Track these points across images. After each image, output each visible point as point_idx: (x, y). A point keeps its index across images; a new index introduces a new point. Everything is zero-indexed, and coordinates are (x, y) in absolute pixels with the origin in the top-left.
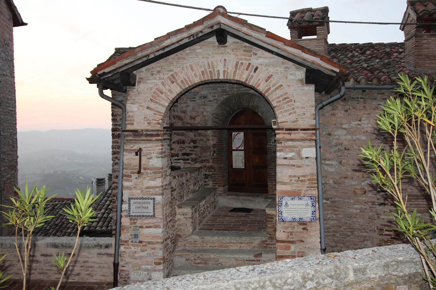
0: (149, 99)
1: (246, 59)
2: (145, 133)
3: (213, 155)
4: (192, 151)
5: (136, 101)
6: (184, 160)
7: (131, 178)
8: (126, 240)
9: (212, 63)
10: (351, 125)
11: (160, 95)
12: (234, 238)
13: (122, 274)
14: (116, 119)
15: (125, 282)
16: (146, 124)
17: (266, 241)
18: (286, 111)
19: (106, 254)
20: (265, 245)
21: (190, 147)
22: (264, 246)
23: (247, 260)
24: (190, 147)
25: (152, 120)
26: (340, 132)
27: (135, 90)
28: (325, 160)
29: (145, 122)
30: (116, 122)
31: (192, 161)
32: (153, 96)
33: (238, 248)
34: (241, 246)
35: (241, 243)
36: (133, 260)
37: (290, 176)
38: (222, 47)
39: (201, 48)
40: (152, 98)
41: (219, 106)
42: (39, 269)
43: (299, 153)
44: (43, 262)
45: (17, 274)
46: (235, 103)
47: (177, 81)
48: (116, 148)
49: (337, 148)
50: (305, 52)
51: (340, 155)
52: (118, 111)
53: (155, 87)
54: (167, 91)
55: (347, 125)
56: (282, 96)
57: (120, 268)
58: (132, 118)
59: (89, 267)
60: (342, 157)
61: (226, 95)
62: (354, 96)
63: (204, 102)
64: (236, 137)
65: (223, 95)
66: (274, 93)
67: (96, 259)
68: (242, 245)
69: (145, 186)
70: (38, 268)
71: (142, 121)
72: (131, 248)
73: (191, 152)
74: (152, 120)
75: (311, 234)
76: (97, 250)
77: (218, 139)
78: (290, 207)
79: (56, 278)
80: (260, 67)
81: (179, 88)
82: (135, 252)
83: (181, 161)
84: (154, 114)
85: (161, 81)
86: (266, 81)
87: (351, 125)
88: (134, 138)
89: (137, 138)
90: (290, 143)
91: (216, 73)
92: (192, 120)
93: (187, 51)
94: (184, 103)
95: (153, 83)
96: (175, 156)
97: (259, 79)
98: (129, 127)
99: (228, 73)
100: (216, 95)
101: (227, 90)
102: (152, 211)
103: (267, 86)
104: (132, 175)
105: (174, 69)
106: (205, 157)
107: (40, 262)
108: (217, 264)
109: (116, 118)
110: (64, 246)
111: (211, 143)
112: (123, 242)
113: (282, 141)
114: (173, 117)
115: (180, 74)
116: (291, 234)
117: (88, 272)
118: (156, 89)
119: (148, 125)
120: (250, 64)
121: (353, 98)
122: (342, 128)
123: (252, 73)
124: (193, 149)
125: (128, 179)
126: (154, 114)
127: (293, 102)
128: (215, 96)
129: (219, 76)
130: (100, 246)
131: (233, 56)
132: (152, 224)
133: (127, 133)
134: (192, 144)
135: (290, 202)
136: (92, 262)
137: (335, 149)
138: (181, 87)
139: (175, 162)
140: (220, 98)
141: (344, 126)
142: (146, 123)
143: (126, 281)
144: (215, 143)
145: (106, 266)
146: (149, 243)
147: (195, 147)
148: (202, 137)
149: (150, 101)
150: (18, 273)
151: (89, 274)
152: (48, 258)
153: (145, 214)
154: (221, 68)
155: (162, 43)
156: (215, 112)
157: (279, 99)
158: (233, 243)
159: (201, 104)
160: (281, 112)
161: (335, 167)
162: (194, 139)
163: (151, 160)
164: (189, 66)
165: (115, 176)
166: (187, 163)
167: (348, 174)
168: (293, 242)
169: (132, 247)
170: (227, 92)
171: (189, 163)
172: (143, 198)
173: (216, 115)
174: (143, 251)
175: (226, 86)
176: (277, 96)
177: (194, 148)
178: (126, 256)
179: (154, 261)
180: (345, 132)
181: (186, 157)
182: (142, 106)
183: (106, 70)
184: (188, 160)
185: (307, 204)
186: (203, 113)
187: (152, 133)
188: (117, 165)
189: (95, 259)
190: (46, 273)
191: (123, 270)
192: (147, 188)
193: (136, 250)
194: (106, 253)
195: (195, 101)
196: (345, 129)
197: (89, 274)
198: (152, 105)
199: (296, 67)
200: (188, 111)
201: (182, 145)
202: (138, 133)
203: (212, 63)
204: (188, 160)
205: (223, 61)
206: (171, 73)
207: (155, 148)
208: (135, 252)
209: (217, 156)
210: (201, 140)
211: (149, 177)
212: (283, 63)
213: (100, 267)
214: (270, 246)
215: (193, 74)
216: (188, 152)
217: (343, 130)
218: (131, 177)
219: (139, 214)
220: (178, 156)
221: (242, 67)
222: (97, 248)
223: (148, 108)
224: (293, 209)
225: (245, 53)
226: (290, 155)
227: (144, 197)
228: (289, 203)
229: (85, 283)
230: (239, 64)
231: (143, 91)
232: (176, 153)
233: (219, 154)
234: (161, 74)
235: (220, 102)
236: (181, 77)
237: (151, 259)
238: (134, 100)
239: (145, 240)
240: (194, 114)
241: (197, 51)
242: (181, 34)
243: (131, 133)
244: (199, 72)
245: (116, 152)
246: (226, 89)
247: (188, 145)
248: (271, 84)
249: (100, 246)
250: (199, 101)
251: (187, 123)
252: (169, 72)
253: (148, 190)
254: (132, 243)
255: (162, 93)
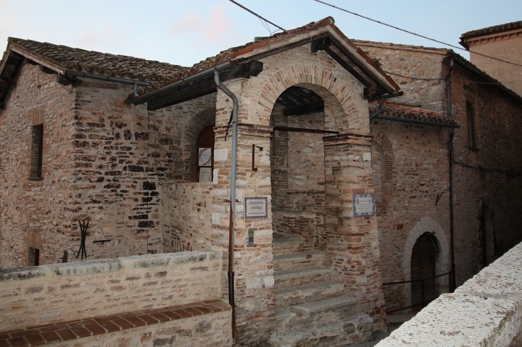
0: (259, 94)
1: (328, 69)
2: (259, 128)
3: (186, 170)
4: (167, 165)
5: (249, 94)
6: (159, 175)
7: (246, 177)
8: (242, 244)
9: (307, 68)
10: (316, 144)
11: (269, 91)
12: (279, 244)
13: (239, 283)
14: (82, 123)
15: (242, 293)
16: (258, 120)
17: (303, 244)
18: (354, 119)
19: (199, 268)
20: (302, 248)
21: (166, 161)
22: (302, 250)
23: (301, 263)
24: (166, 161)
25: (263, 116)
26: (306, 150)
27: (248, 83)
28: (296, 174)
29: (257, 117)
30: (81, 127)
31: (167, 176)
32: (263, 92)
33: (282, 254)
34: (284, 252)
35: (285, 249)
36: (248, 267)
37: (358, 176)
38: (314, 54)
39: (299, 52)
40: (262, 94)
41: (193, 119)
42: (123, 298)
43: (362, 157)
44: (128, 288)
45: (93, 309)
46: (212, 117)
47: (282, 79)
48: (79, 159)
49: (305, 164)
50: (378, 71)
51: (308, 170)
52: (83, 114)
53: (265, 83)
54: (274, 88)
55: (313, 144)
56: (351, 106)
57: (236, 277)
58: (247, 111)
59: (181, 286)
60: (311, 172)
61: (202, 108)
62: (318, 120)
63: (179, 113)
64: (203, 153)
65: (198, 107)
66: (347, 103)
67: (189, 275)
68: (285, 250)
69: (257, 185)
70: (121, 297)
71: (255, 116)
72: (246, 253)
73: (166, 167)
74: (263, 116)
75: (373, 226)
76: (191, 265)
77: (191, 153)
78: (360, 203)
79: (144, 307)
80: (338, 78)
81: (283, 87)
82: (250, 258)
83: (156, 177)
84: (265, 110)
85: (270, 77)
86: (342, 91)
87: (316, 144)
88: (248, 134)
89: (251, 134)
90: (356, 148)
91: (310, 77)
92: (168, 132)
93: (290, 53)
94: (160, 112)
95: (263, 78)
96: (150, 171)
97: (337, 89)
98: (244, 121)
99: (317, 79)
100: (192, 107)
101: (203, 103)
102: (264, 211)
103: (342, 95)
104: (247, 173)
105: (280, 67)
106: (178, 173)
107: (125, 288)
108: (278, 270)
109: (81, 121)
110: (155, 263)
111: (184, 158)
112: (240, 247)
113: (352, 145)
114: (148, 126)
115: (284, 73)
116: (361, 228)
117: (180, 293)
118: (266, 85)
119: (259, 120)
120: (331, 74)
121: (317, 121)
122: (309, 147)
123: (333, 83)
124: (168, 163)
125: (243, 177)
126: (265, 110)
127: (357, 112)
128: (191, 108)
129: (312, 81)
130: (194, 259)
131: (321, 65)
132: (264, 225)
133: (243, 127)
134: (167, 157)
135: (360, 199)
136: (185, 280)
137: (304, 165)
138: (285, 86)
139: (149, 178)
140: (195, 111)
141: (310, 145)
142: (258, 118)
143: (243, 291)
144: (187, 157)
145: (199, 282)
146: (263, 246)
147: (170, 161)
148: (176, 151)
149: (261, 96)
150: (95, 309)
151: (181, 296)
152: (135, 282)
153: (259, 215)
154: (312, 73)
155: (289, 40)
156: (188, 125)
157: (349, 109)
158: (278, 249)
159: (176, 115)
160: (351, 120)
161: (304, 181)
162: (169, 152)
163: (261, 158)
164: (290, 67)
165: (77, 194)
166: (162, 179)
167: (314, 186)
168: (362, 235)
169: (247, 252)
170: (203, 105)
171: (164, 179)
172: (256, 198)
173: (190, 128)
174: (257, 255)
175: (202, 99)
176: (348, 106)
177: (169, 162)
178: (242, 261)
179: (267, 265)
180: (311, 150)
181: (161, 172)
182: (255, 100)
183: (245, 56)
184: (163, 175)
185: (370, 201)
186: (177, 125)
187: (264, 129)
188: (80, 181)
189: (187, 276)
190: (131, 302)
191: (240, 280)
192: (260, 187)
193: (251, 255)
194: (199, 266)
195: (171, 111)
196: (311, 147)
197: (181, 296)
198: (263, 101)
199: (358, 83)
200: (164, 121)
201: (157, 158)
202: (253, 128)
203: (307, 68)
204: (163, 175)
205: (314, 67)
206: (278, 71)
207: (265, 145)
208: (250, 258)
209: (190, 172)
210: (176, 154)
211: (261, 175)
212: (351, 78)
213: (193, 284)
214: (306, 248)
215: (294, 75)
216: (163, 166)
217: (309, 149)
218: (245, 174)
219: (254, 215)
220: (152, 171)
221: (327, 76)
222: (191, 262)
223: (259, 103)
224: (362, 205)
225: (328, 64)
226: (357, 158)
227: (258, 196)
228: (359, 200)
229: (180, 306)
230: (325, 73)
231: (255, 85)
232: (150, 167)
233: (192, 169)
234: (269, 70)
235: (195, 115)
236: (285, 76)
237: (264, 264)
238: (248, 93)
239: (259, 244)
240: (169, 125)
241: (296, 54)
242: (303, 35)
243: (247, 128)
244: (298, 74)
245: (80, 164)
246: (202, 102)
247: (163, 159)
248: (345, 95)
249: (194, 259)
250: (175, 112)
251: (163, 135)
252: (275, 70)
253: (260, 189)
254: (247, 248)
255: (270, 89)
